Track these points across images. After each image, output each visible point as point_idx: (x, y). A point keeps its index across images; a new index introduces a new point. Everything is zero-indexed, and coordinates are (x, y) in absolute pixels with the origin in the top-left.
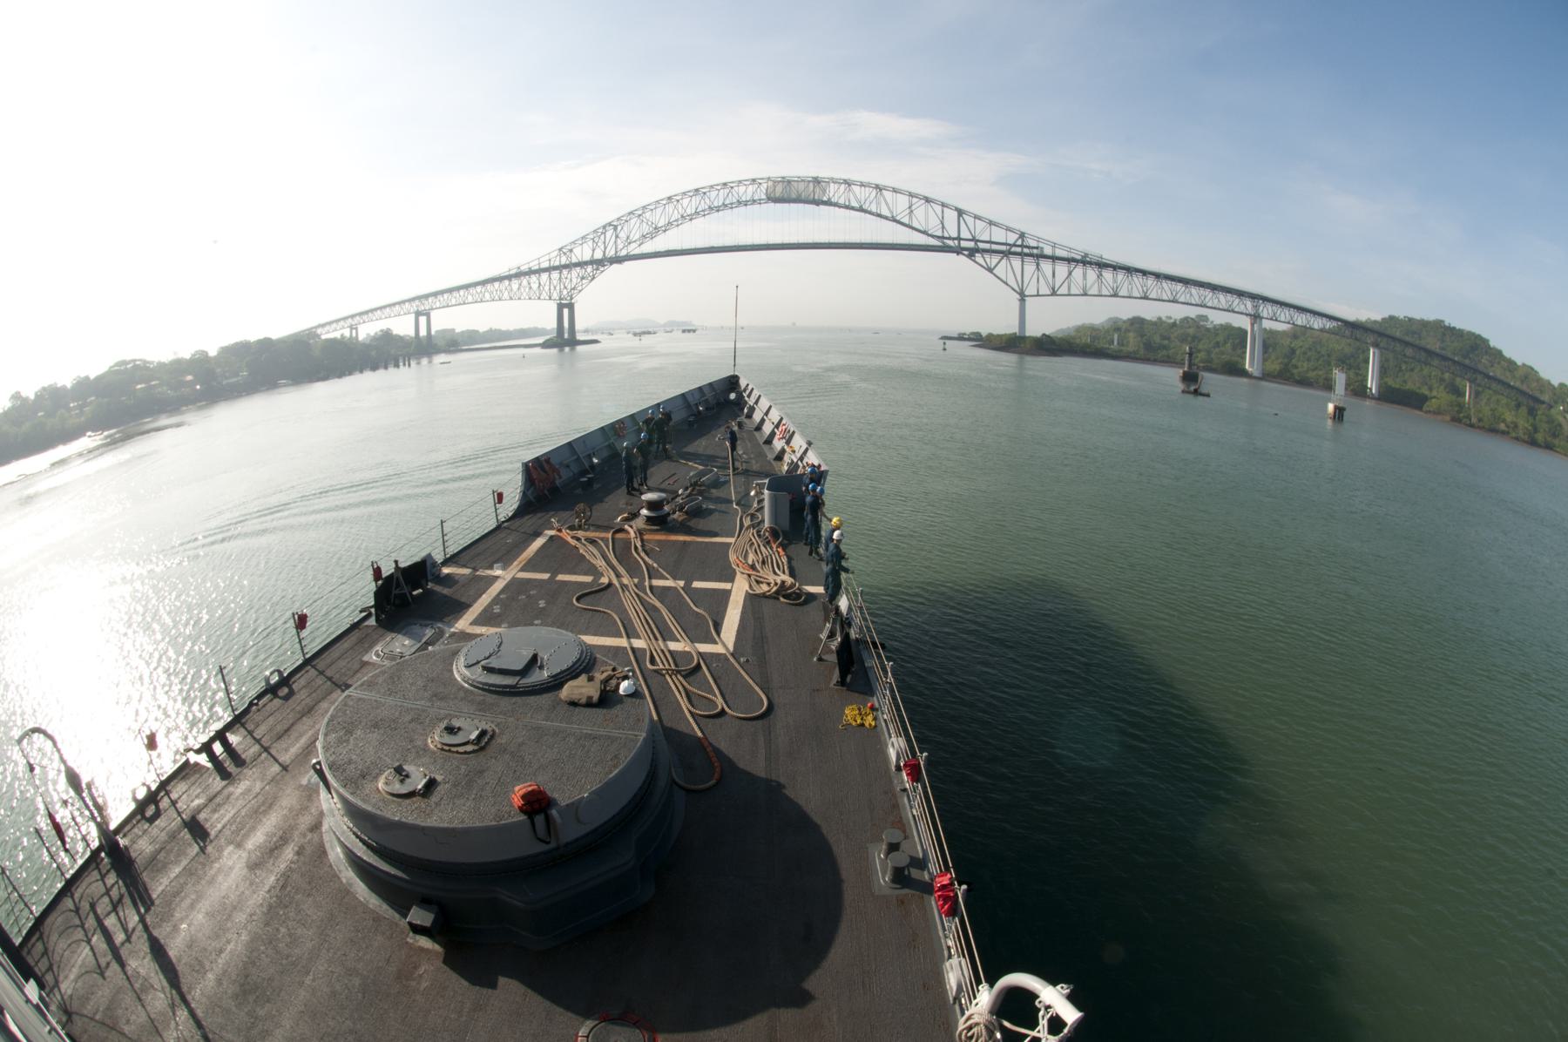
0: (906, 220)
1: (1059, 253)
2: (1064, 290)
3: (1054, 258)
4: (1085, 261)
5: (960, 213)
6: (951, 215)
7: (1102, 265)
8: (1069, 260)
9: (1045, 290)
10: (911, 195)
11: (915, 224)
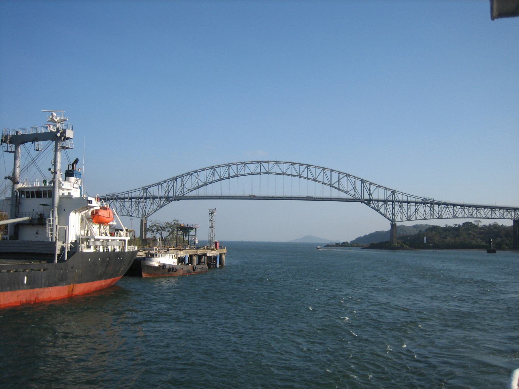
0: (336, 185)
1: (413, 199)
2: (414, 218)
3: (408, 202)
4: (424, 202)
5: (362, 181)
6: (358, 184)
7: (433, 203)
8: (416, 203)
9: (404, 219)
10: (340, 173)
11: (341, 188)
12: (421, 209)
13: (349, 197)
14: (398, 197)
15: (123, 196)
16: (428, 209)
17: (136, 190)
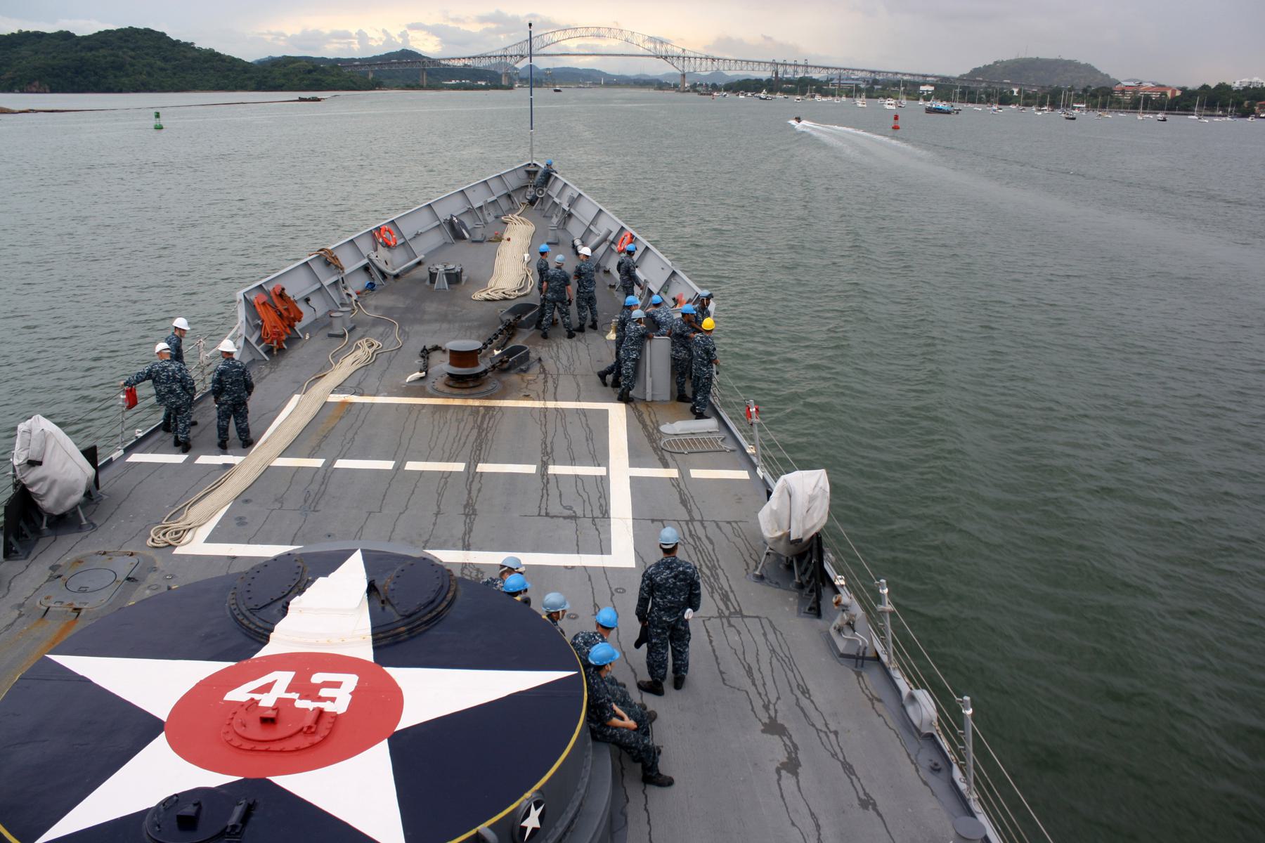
1: (698, 55)
12: (704, 63)
13: (652, 54)
14: (688, 54)
15: (489, 55)
16: (709, 62)
17: (498, 50)
